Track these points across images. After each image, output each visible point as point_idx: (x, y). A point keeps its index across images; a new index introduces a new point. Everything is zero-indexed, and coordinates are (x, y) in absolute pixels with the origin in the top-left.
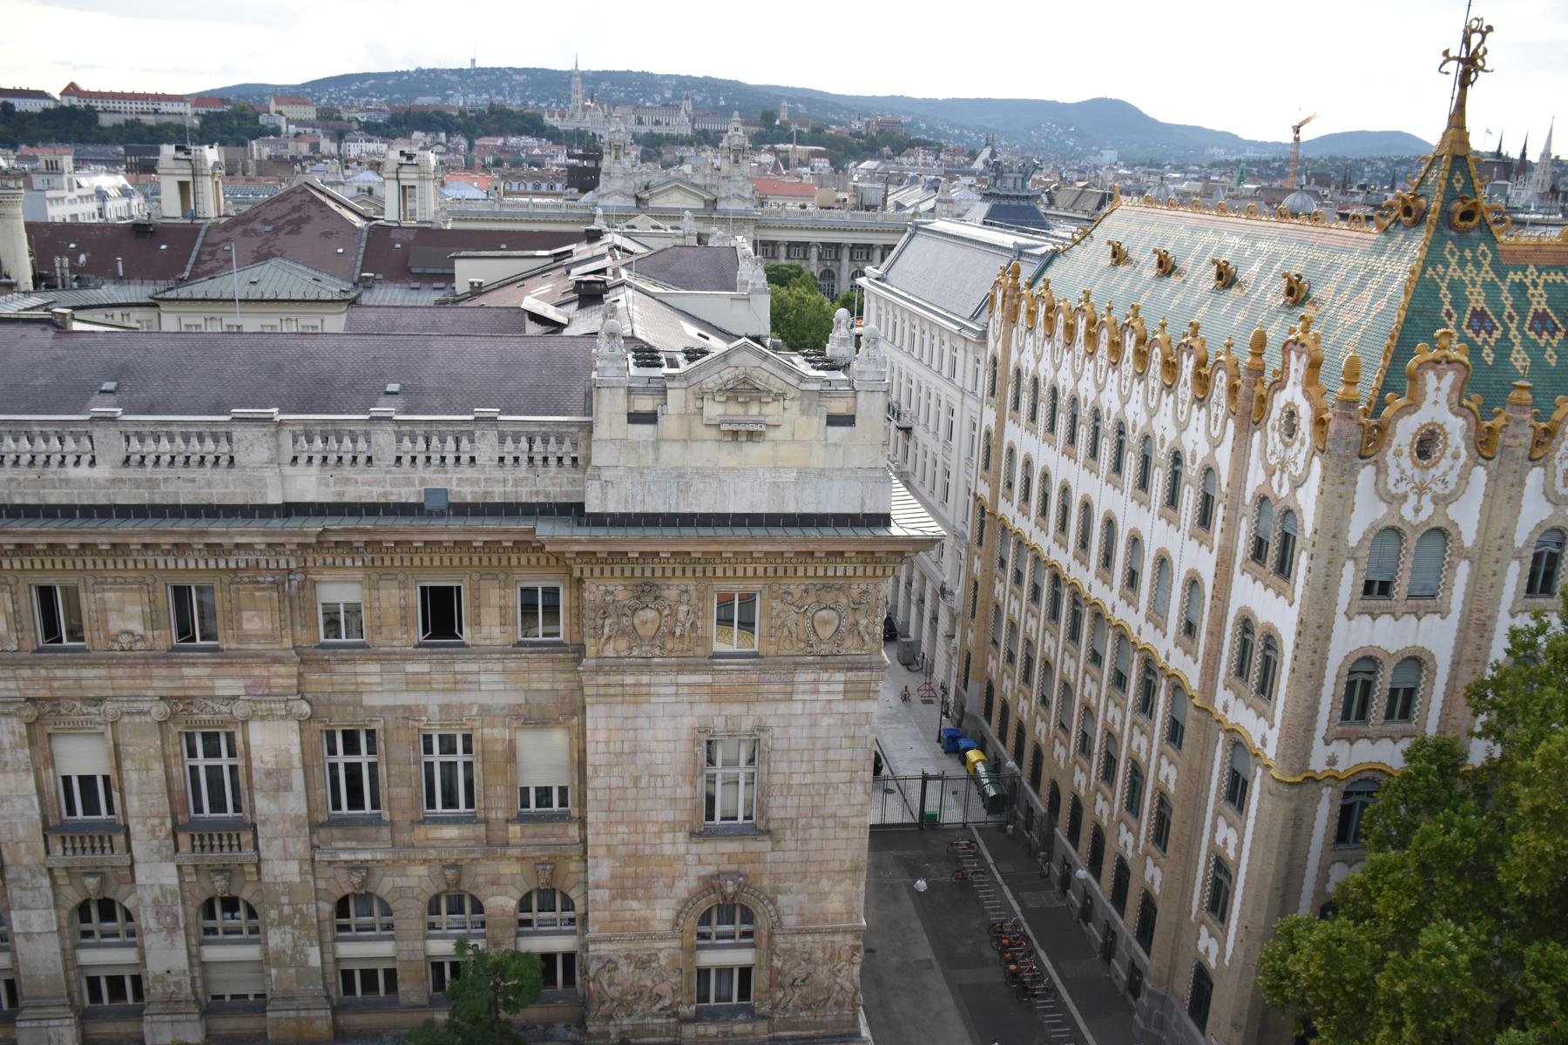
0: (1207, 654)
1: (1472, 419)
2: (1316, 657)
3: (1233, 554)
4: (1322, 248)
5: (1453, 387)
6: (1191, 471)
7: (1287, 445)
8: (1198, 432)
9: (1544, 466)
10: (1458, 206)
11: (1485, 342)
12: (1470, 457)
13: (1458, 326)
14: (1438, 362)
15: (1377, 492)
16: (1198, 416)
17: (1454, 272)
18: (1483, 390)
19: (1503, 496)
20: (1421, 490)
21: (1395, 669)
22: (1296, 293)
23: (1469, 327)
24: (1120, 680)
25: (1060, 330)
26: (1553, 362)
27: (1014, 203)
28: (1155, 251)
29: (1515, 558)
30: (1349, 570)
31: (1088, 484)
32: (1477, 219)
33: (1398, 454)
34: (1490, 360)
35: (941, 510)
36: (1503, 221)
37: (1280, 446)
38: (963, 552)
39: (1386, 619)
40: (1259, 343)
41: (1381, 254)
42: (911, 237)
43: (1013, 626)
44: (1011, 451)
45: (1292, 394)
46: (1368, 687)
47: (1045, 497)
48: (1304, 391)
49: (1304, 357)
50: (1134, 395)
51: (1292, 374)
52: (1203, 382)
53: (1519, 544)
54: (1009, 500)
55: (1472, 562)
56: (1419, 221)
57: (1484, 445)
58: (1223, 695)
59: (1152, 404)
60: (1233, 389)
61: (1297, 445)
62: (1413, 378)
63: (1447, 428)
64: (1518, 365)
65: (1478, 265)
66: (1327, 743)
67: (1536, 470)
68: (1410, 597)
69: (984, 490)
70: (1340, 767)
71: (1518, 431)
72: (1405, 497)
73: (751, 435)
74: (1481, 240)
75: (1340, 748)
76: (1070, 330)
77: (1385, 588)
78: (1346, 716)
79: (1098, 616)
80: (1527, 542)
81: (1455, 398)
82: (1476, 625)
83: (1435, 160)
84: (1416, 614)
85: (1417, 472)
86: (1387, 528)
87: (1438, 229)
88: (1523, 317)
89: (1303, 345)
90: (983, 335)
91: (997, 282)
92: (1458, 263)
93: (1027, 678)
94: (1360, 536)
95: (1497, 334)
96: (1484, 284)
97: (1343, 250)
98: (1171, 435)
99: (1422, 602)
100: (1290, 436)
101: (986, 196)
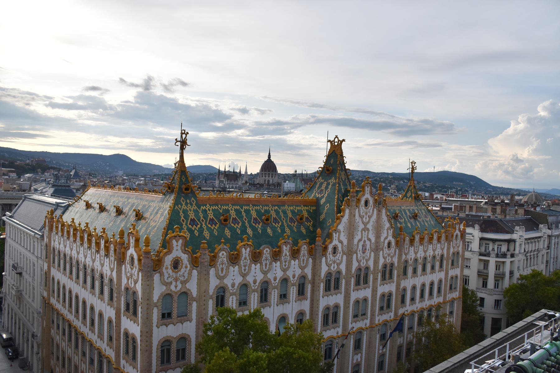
0: (116, 348)
2: (147, 343)
3: (120, 310)
4: (147, 201)
6: (106, 281)
7: (132, 269)
8: (105, 266)
9: (215, 267)
10: (184, 186)
11: (195, 229)
12: (191, 267)
13: (186, 224)
14: (176, 237)
15: (161, 282)
18: (193, 245)
19: (204, 279)
20: (176, 280)
21: (177, 342)
22: (139, 216)
23: (190, 224)
24: (92, 361)
27: (64, 188)
30: (155, 311)
32: (190, 190)
37: (130, 269)
38: (40, 319)
39: (171, 326)
40: (122, 233)
41: (162, 202)
42: (23, 201)
43: (58, 346)
44: (53, 279)
46: (169, 351)
48: (135, 250)
50: (88, 255)
51: (131, 244)
52: (107, 249)
53: (211, 294)
54: (54, 297)
55: (197, 302)
56: (172, 191)
57: (195, 263)
58: (123, 362)
59: (94, 258)
60: (115, 250)
62: (168, 243)
64: (206, 236)
65: (191, 204)
68: (178, 317)
69: (45, 294)
71: (205, 257)
72: (171, 283)
74: (192, 197)
77: (169, 315)
78: (162, 362)
79: (83, 338)
81: (183, 248)
83: (176, 172)
84: (181, 322)
85: (174, 274)
86: (167, 294)
87: (178, 193)
90: (42, 236)
91: (46, 217)
93: (64, 366)
94: (157, 298)
95: (199, 226)
97: (152, 201)
101: (53, 186)
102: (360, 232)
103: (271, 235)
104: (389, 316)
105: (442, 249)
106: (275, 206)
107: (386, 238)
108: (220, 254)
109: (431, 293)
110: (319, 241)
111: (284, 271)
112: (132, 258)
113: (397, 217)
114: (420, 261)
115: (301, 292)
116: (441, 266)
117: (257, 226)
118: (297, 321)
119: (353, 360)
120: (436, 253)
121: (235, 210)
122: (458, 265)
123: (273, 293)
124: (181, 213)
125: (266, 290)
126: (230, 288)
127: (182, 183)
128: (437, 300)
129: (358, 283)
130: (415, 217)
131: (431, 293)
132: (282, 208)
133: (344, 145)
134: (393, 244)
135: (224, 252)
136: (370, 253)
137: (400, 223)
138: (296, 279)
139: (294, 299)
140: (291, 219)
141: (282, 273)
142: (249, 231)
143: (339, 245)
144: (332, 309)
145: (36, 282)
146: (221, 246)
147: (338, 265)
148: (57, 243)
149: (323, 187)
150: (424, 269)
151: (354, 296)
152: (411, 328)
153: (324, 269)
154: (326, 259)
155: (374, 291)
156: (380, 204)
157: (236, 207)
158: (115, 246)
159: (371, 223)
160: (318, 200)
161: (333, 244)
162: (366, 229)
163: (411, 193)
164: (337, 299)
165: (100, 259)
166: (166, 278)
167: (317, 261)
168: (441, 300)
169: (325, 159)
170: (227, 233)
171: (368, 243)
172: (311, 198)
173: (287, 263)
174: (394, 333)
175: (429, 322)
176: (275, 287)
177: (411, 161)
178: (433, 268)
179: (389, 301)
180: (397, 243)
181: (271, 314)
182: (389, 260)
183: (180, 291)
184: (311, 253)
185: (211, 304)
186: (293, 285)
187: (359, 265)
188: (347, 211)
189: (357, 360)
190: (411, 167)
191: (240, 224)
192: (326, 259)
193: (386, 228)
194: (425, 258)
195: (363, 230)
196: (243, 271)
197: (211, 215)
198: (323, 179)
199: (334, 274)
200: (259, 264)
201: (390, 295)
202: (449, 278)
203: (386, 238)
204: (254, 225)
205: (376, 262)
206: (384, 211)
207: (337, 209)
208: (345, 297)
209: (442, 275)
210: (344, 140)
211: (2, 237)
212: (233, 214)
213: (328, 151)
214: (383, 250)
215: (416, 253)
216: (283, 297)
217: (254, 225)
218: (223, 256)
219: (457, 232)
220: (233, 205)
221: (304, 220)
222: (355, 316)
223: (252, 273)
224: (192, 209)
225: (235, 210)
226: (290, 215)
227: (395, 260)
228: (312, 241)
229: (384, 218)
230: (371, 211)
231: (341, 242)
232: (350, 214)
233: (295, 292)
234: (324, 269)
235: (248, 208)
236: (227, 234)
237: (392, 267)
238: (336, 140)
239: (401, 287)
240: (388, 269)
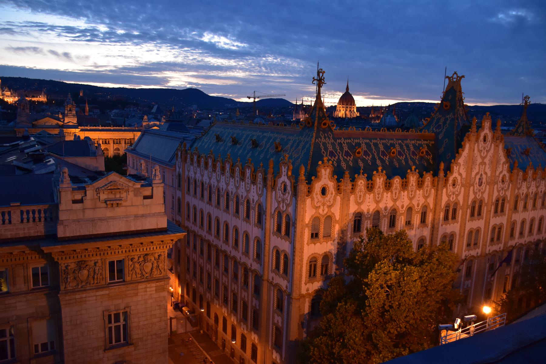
5: (329, 173)
7: (284, 195)
12: (336, 194)
16: (253, 188)
19: (345, 204)
20: (324, 205)
25: (202, 164)
26: (351, 165)
33: (316, 194)
34: (336, 165)
37: (282, 195)
39: (318, 244)
46: (315, 265)
50: (231, 183)
51: (283, 173)
57: (338, 189)
61: (287, 194)
65: (329, 138)
66: (306, 284)
68: (324, 237)
70: (310, 292)
72: (320, 206)
73: (338, 189)
75: (309, 285)
81: (330, 177)
95: (337, 158)
98: (245, 194)
103: (397, 166)
106: (399, 140)
107: (501, 172)
110: (442, 174)
111: (411, 199)
121: (366, 143)
124: (321, 146)
125: (394, 217)
129: (472, 215)
132: (405, 142)
133: (463, 83)
136: (486, 187)
138: (420, 207)
141: (409, 202)
143: (459, 178)
147: (457, 196)
149: (441, 123)
153: (445, 199)
154: (447, 190)
157: (366, 141)
159: (488, 157)
161: (453, 176)
164: (453, 227)
166: (315, 203)
167: (439, 192)
171: (484, 176)
173: (413, 193)
181: (413, 234)
183: (326, 214)
186: (417, 212)
188: (467, 146)
189: (468, 285)
191: (371, 156)
192: (447, 190)
193: (502, 163)
195: (481, 163)
197: (346, 148)
199: (453, 205)
204: (382, 157)
206: (501, 146)
208: (461, 226)
210: (463, 77)
213: (446, 87)
214: (497, 184)
215: (528, 188)
217: (382, 157)
220: (363, 139)
221: (425, 153)
222: (468, 245)
225: (366, 143)
227: (508, 194)
230: (489, 146)
231: (460, 174)
232: (470, 148)
233: (418, 219)
234: (445, 199)
235: (376, 141)
238: (455, 76)
240: (500, 202)
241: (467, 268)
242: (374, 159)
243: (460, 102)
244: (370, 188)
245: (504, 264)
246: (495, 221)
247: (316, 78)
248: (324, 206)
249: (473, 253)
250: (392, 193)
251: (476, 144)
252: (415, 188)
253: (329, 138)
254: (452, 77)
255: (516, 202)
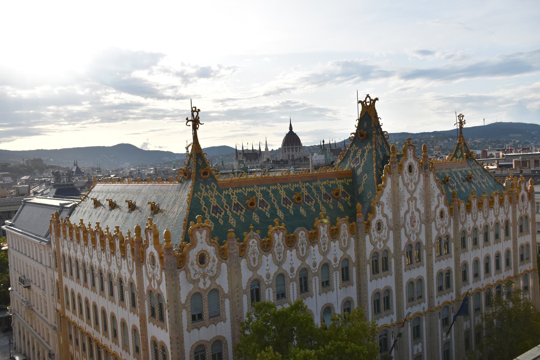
1: (216, 246)
3: (145, 315)
5: (206, 236)
6: (126, 285)
7: (153, 269)
8: (123, 269)
9: (245, 258)
12: (219, 260)
13: (209, 213)
14: (199, 228)
15: (188, 281)
17: (204, 194)
18: (219, 235)
20: (204, 276)
22: (155, 209)
28: (107, 200)
29: (244, 293)
31: (94, 297)
32: (209, 174)
34: (222, 223)
35: (46, 319)
36: (218, 174)
37: (151, 270)
39: (203, 329)
40: (138, 230)
44: (66, 289)
45: (151, 249)
47: (81, 305)
49: (152, 234)
51: (150, 241)
52: (123, 249)
53: (244, 288)
54: (69, 309)
55: (229, 299)
56: (189, 178)
57: (223, 254)
60: (133, 250)
61: (156, 268)
62: (192, 235)
63: (208, 251)
64: (232, 223)
65: (212, 190)
67: (243, 260)
68: (210, 317)
69: (59, 307)
72: (199, 280)
76: (78, 236)
77: (200, 316)
79: (107, 352)
80: (247, 287)
82: (237, 321)
84: (214, 323)
85: (201, 269)
86: (195, 293)
87: (196, 179)
88: (231, 207)
89: (151, 229)
90: (49, 243)
91: (51, 221)
92: (205, 190)
94: (185, 299)
95: (223, 213)
96: (215, 197)
99: (215, 318)
100: (154, 265)
101: (55, 186)
102: (405, 203)
103: (305, 215)
104: (450, 297)
105: (507, 214)
106: (306, 182)
107: (437, 207)
108: (251, 243)
109: (498, 267)
110: (360, 217)
111: (324, 254)
112: (153, 257)
113: (447, 181)
114: (481, 230)
115: (346, 277)
116: (507, 234)
117: (288, 208)
118: (345, 310)
119: (413, 350)
120: (500, 219)
121: (262, 192)
122: (528, 230)
123: (313, 281)
125: (306, 278)
126: (265, 279)
127: (198, 165)
128: (505, 274)
130: (469, 179)
131: (498, 267)
132: (314, 184)
133: (377, 105)
134: (446, 212)
135: (254, 240)
136: (421, 226)
137: (453, 188)
138: (338, 262)
139: (338, 286)
140: (325, 195)
141: (322, 257)
142: (280, 213)
144: (382, 293)
145: (47, 295)
146: (251, 233)
147: (385, 242)
148: (66, 249)
149: (358, 155)
150: (486, 239)
151: (407, 276)
152: (478, 309)
153: (369, 249)
154: (370, 236)
155: (430, 269)
156: (426, 168)
157: (262, 188)
158: (132, 245)
159: (418, 191)
160: (354, 171)
161: (377, 219)
162: (412, 199)
163: (462, 151)
164: (386, 282)
165: (117, 262)
168: (511, 273)
169: (356, 123)
170: (256, 218)
171: (416, 214)
172: (346, 169)
173: (326, 246)
174: (459, 317)
175: (499, 300)
176: (316, 274)
177: (458, 114)
178: (497, 236)
179: (448, 280)
180: (451, 211)
181: (314, 304)
182: (443, 232)
183: (210, 288)
184: (353, 231)
185: (246, 299)
186: (336, 269)
187: (409, 240)
188: (389, 180)
189: (418, 350)
190: (458, 121)
191: (269, 207)
192: (370, 236)
193: (436, 195)
194: (487, 227)
195: (409, 199)
196: (278, 259)
197: (235, 200)
198: (356, 146)
199: (381, 254)
200: (295, 250)
201: (449, 272)
202: (518, 247)
203: (437, 207)
204: (284, 206)
205: (428, 235)
206: (432, 176)
207: (377, 179)
209: (509, 244)
210: (377, 99)
211: (3, 248)
212: (260, 196)
215: (475, 221)
216: (326, 284)
217: (284, 206)
218: (253, 244)
219: (523, 192)
220: (258, 186)
221: (340, 194)
222: (411, 299)
223: (288, 260)
224: (213, 195)
225: (262, 192)
226: (324, 191)
227: (451, 231)
228: (353, 218)
229: (433, 183)
233: (338, 277)
234: (369, 249)
235: (275, 187)
236: (255, 219)
237: (448, 239)
238: (368, 100)
239: (461, 262)
241: (414, 328)
242: (273, 209)
243: (377, 130)
244: (266, 246)
245: (461, 318)
246: (439, 266)
247: (190, 118)
248: (204, 278)
249: (417, 309)
250: (297, 249)
251: (400, 177)
252: (327, 239)
253: (212, 190)
254: (365, 101)
255: (464, 240)
